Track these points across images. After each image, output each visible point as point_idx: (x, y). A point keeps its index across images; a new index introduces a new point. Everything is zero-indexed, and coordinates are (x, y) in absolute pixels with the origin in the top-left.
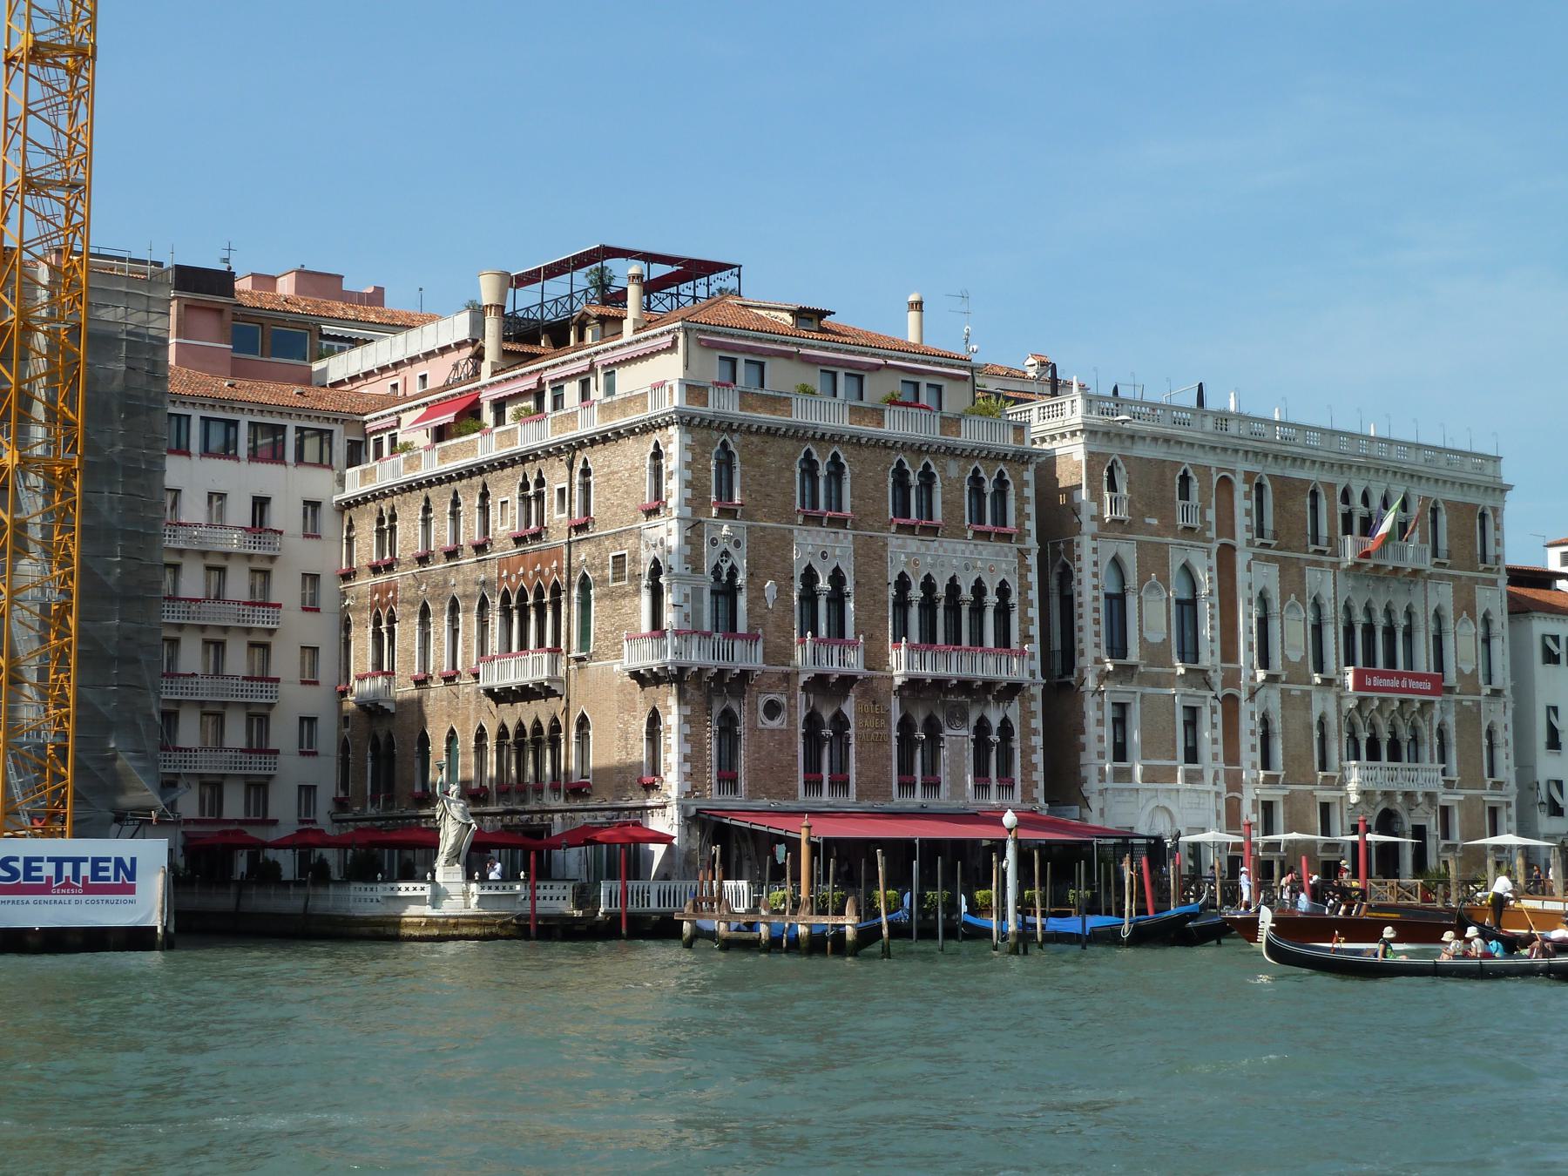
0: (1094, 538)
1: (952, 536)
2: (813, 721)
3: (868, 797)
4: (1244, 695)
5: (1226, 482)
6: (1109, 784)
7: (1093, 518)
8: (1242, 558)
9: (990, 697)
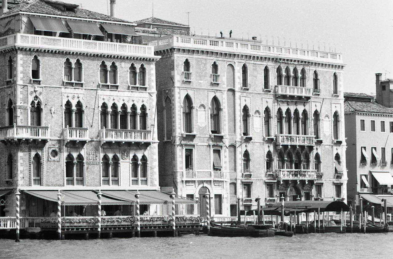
2: (70, 157)
7: (179, 81)
8: (237, 94)
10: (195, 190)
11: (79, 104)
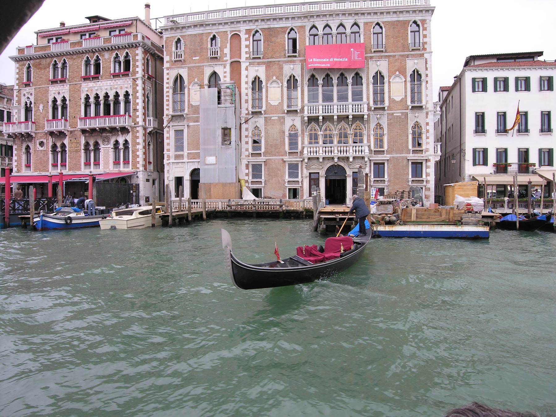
0: (168, 69)
1: (106, 78)
2: (54, 146)
3: (73, 170)
5: (236, 36)
6: (172, 160)
7: (167, 62)
8: (243, 66)
9: (120, 133)
11: (64, 100)
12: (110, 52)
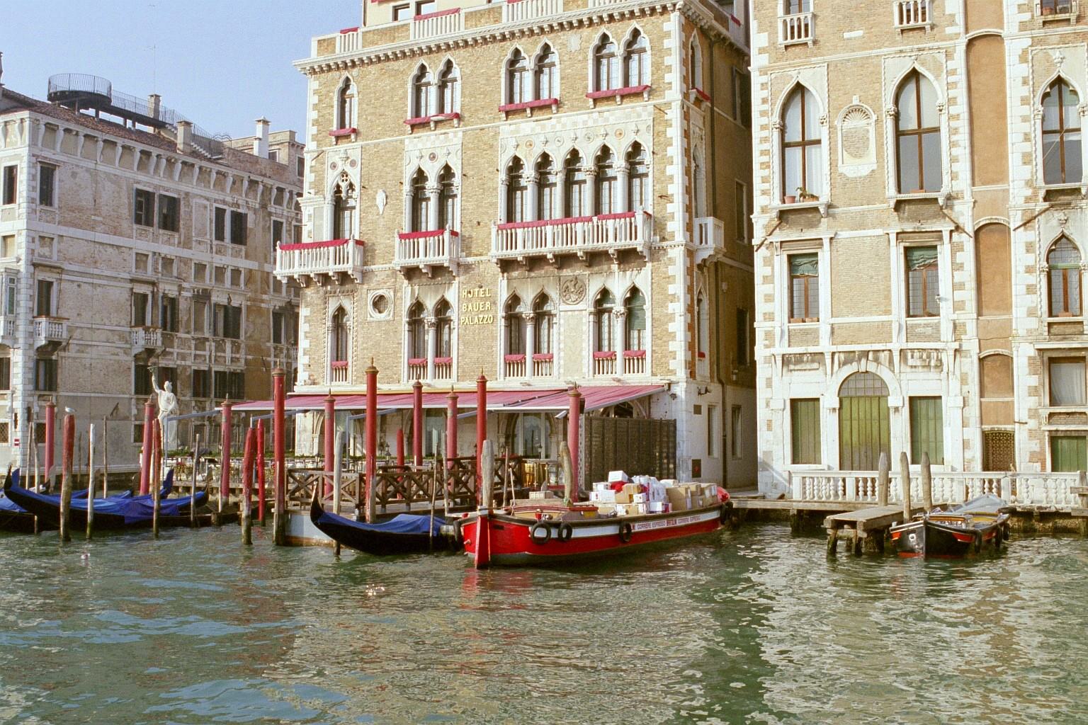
1: (573, 108)
4: (1015, 220)
7: (762, 51)
8: (1014, 46)
9: (615, 267)
10: (823, 386)
11: (447, 173)
12: (586, 31)
